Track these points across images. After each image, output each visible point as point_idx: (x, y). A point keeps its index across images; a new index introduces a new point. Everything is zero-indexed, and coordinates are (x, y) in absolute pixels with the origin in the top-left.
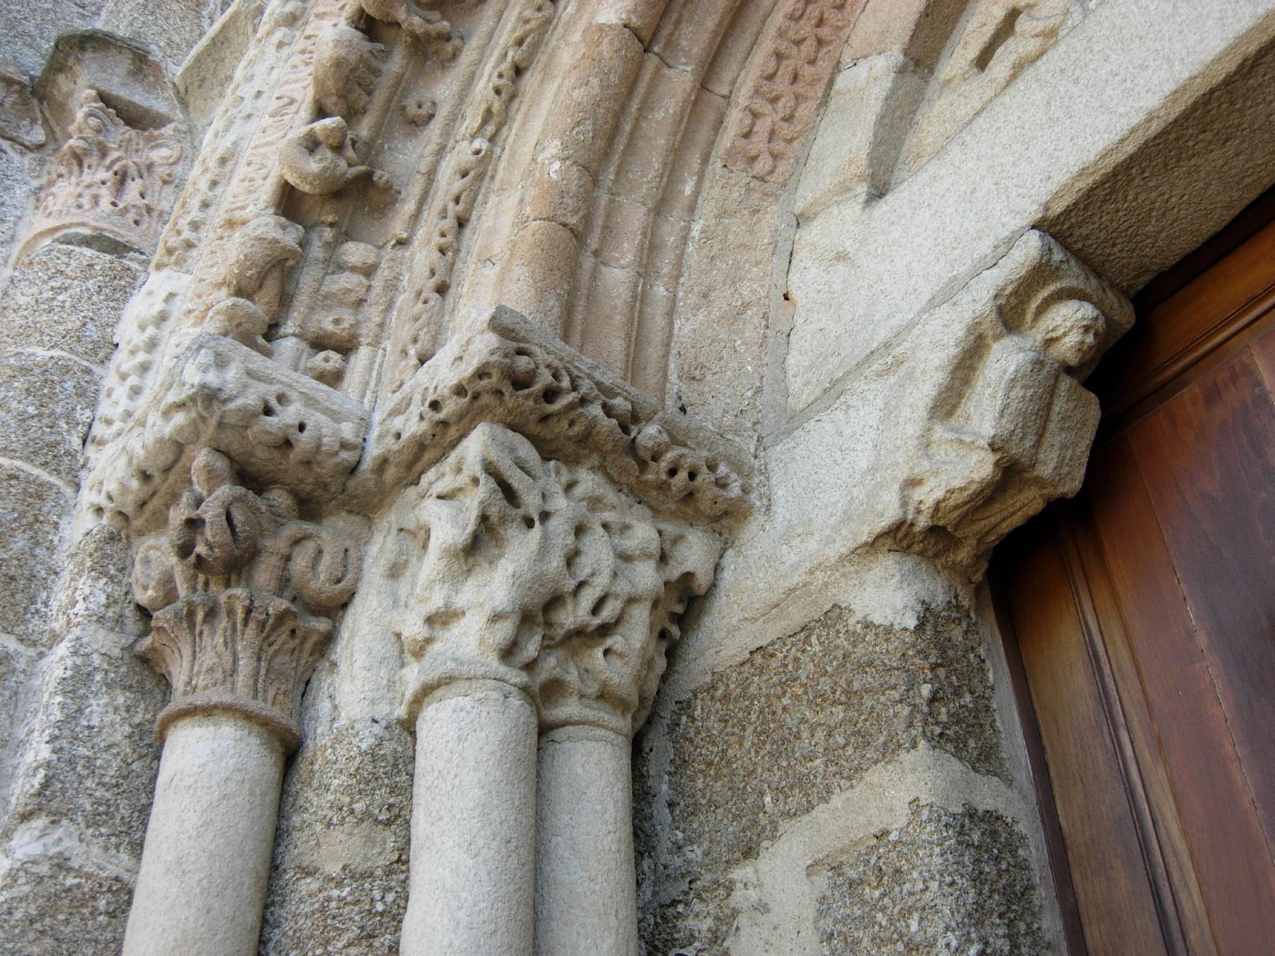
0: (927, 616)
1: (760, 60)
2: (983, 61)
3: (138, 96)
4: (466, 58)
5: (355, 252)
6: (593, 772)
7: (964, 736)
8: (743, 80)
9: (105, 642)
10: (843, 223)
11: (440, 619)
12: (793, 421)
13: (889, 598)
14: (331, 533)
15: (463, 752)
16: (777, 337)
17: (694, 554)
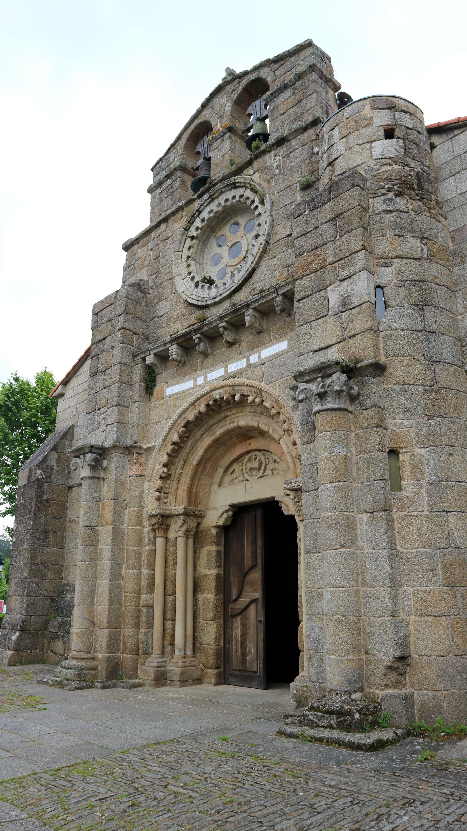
0: (217, 533)
1: (211, 463)
2: (232, 473)
3: (140, 452)
4: (179, 457)
5: (168, 482)
6: (191, 541)
7: (218, 544)
8: (208, 465)
9: (150, 528)
10: (215, 487)
11: (179, 531)
12: (209, 509)
13: (214, 531)
14: (169, 520)
15: (181, 543)
16: (209, 497)
17: (200, 520)
